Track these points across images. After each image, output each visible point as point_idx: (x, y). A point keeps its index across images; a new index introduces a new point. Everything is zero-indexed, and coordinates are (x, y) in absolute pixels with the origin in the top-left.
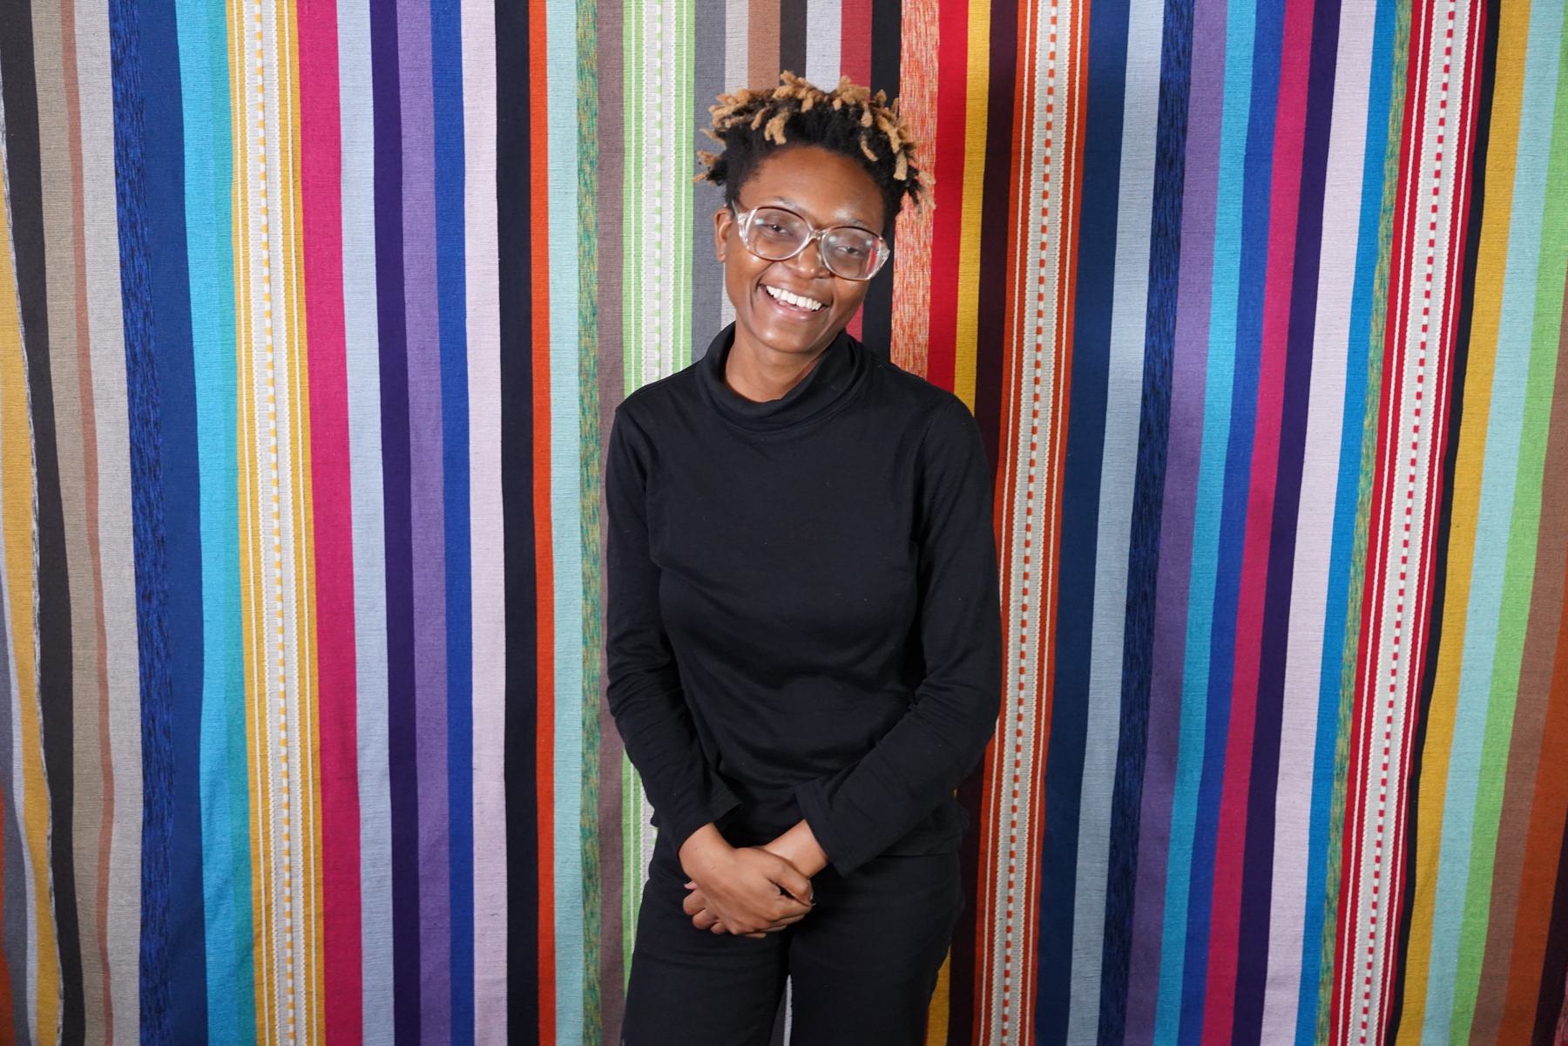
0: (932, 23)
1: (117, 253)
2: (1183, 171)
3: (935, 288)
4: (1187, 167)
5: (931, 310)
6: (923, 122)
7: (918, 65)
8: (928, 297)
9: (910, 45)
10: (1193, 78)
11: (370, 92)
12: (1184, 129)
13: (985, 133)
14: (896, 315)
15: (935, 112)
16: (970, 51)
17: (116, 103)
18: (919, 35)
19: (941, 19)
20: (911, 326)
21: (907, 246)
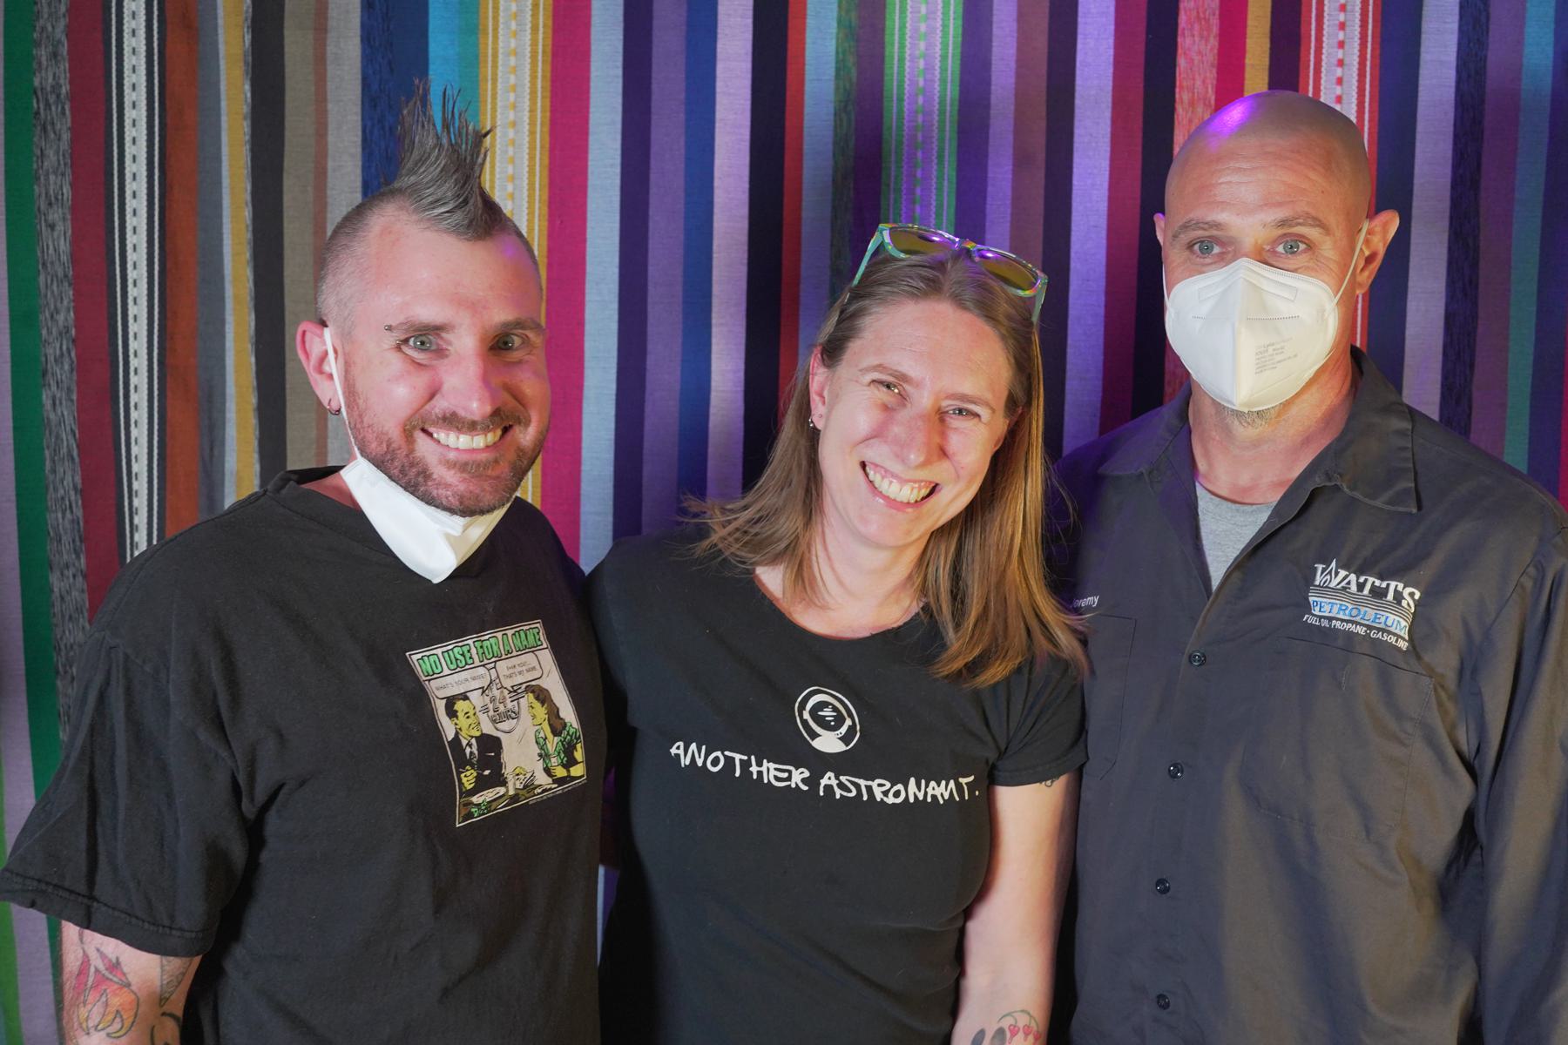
2: (1470, 408)
4: (1474, 405)
10: (1481, 314)
11: (615, 306)
12: (1472, 366)
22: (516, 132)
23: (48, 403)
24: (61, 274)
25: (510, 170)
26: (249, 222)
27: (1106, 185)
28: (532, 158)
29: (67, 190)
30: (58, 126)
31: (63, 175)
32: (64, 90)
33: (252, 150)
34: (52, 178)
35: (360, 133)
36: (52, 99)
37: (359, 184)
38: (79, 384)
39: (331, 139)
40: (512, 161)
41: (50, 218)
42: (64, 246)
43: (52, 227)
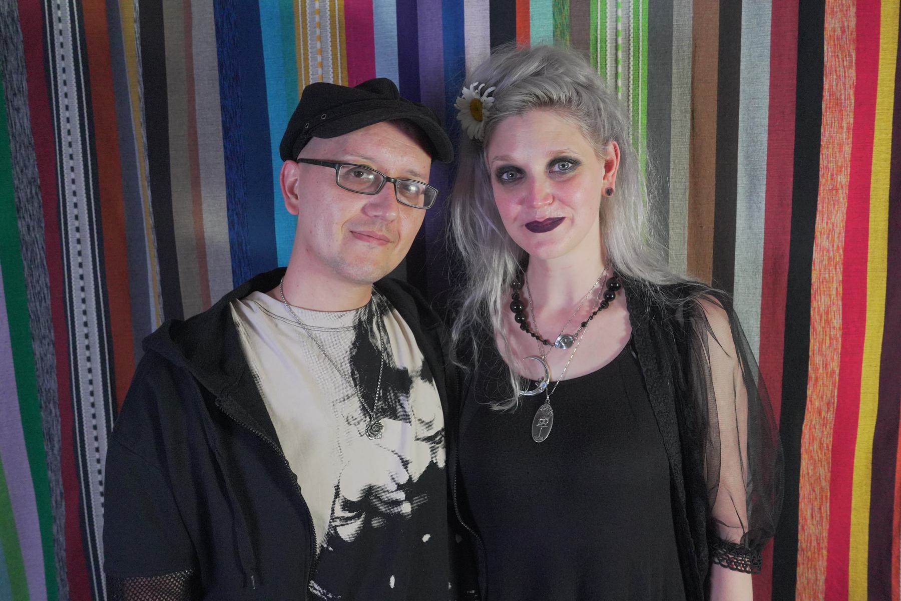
0: (850, 67)
1: (230, 264)
3: (846, 282)
5: (843, 299)
6: (841, 148)
7: (838, 102)
8: (841, 290)
9: (831, 87)
13: (889, 157)
14: (814, 304)
15: (850, 140)
16: (879, 89)
17: (226, 158)
18: (839, 77)
19: (857, 64)
20: (827, 313)
21: (822, 249)
22: (321, 18)
23: (24, 230)
24: (26, 141)
25: (319, 45)
26: (141, 96)
27: (769, 23)
28: (333, 36)
29: (25, 84)
30: (15, 40)
31: (22, 74)
32: (16, 14)
33: (142, 45)
34: (14, 76)
35: (214, 27)
36: (9, 21)
37: (216, 64)
38: (45, 216)
39: (194, 33)
40: (320, 38)
41: (15, 103)
42: (27, 123)
43: (18, 110)
